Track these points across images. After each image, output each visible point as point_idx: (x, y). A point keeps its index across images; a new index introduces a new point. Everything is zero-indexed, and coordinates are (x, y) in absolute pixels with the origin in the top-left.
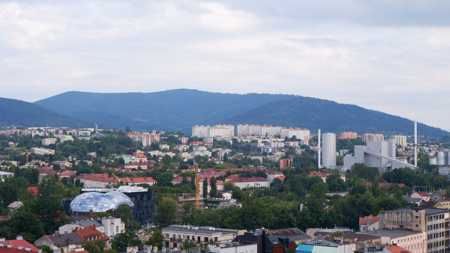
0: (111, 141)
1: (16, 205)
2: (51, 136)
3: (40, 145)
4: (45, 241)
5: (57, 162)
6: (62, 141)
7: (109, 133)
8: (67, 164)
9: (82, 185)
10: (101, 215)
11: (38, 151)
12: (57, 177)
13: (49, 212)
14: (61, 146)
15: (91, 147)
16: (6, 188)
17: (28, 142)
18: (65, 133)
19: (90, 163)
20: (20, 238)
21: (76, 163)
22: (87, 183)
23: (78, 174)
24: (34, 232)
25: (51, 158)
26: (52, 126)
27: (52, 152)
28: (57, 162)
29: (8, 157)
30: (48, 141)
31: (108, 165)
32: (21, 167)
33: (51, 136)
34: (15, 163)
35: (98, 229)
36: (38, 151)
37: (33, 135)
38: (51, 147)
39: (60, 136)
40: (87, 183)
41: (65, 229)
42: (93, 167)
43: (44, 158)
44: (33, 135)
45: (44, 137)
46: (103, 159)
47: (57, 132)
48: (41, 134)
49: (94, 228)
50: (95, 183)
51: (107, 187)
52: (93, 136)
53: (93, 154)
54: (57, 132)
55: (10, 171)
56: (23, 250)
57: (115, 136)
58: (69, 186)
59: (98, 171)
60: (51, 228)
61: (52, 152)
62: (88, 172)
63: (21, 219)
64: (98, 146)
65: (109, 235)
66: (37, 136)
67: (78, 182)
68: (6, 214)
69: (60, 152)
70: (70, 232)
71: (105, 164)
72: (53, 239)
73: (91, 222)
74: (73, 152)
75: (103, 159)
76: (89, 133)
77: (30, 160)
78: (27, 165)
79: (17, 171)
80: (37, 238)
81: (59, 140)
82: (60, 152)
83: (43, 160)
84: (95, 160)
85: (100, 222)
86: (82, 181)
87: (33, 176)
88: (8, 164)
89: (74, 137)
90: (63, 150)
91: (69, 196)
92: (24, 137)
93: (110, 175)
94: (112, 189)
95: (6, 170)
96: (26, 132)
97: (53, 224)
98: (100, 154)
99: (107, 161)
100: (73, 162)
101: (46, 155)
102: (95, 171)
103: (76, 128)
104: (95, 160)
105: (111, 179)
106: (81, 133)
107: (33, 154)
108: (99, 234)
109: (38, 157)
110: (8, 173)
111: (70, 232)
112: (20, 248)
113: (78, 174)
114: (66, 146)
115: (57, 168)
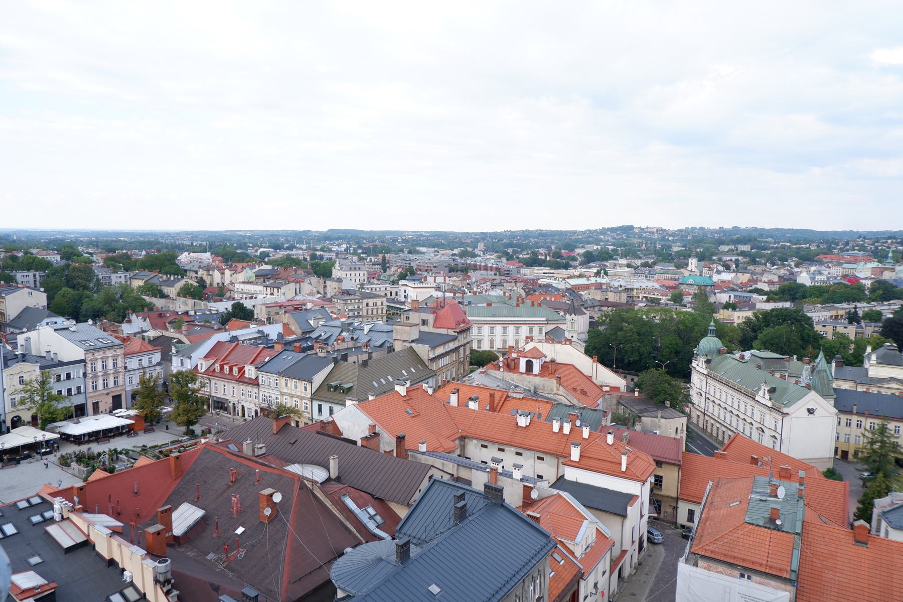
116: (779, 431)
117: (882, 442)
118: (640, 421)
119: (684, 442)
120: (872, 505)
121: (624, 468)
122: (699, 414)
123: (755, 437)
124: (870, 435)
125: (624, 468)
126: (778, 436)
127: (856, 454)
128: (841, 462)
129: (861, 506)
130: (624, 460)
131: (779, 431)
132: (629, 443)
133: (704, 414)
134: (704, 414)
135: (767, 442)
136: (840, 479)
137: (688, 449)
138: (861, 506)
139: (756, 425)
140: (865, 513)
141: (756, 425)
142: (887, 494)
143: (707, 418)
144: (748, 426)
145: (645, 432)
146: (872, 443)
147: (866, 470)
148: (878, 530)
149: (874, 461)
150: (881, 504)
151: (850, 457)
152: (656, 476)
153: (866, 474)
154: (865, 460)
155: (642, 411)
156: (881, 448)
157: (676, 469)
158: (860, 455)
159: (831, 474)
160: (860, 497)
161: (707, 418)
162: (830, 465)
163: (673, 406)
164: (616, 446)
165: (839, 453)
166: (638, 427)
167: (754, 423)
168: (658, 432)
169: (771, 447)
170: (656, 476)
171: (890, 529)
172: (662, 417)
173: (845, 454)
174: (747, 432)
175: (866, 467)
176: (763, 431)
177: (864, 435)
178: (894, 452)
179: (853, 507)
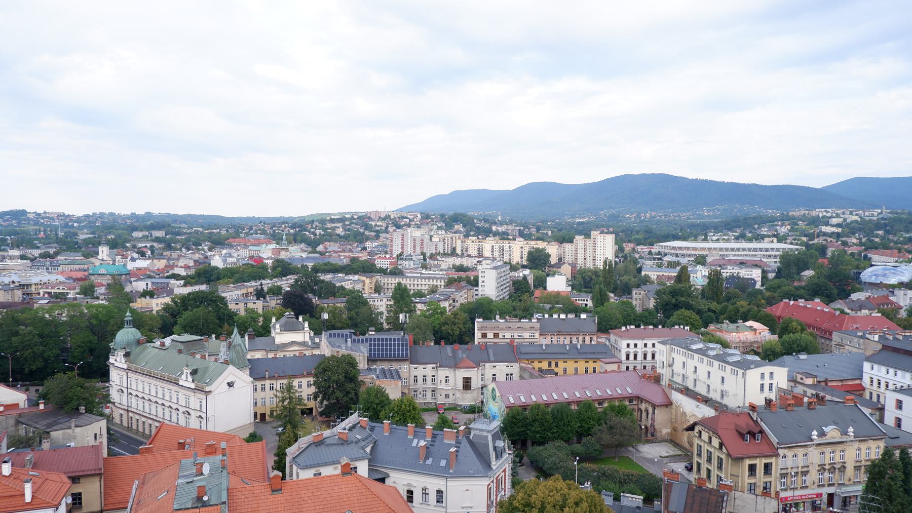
0: (900, 220)
1: (808, 273)
2: (838, 216)
3: (827, 224)
4: (839, 304)
5: (844, 239)
6: (849, 221)
7: (897, 213)
8: (854, 241)
9: (870, 259)
10: (893, 286)
11: (825, 229)
12: (845, 251)
13: (840, 281)
14: (848, 225)
15: (878, 226)
16: (798, 260)
17: (816, 222)
18: (851, 213)
19: (877, 240)
20: (817, 300)
21: (863, 240)
22: (875, 258)
23: (866, 250)
24: (828, 296)
25: (838, 236)
26: (839, 208)
27: (839, 230)
28: (844, 239)
29: (798, 233)
30: (835, 221)
31: (896, 243)
32: (811, 243)
33: (836, 218)
34: (805, 239)
35: (891, 298)
36: (825, 229)
37: (821, 215)
38: (838, 225)
39: (846, 217)
40: (875, 258)
41: (854, 296)
42: (880, 244)
43: (832, 235)
44: (821, 215)
45: (832, 217)
46: (891, 237)
47: (844, 213)
48: (829, 215)
49: (887, 297)
50: (883, 258)
51: (896, 262)
52: (880, 216)
53: (881, 232)
54: (844, 213)
55: (800, 245)
56: (822, 311)
57: (904, 216)
58: (858, 260)
59: (886, 247)
60: (845, 294)
61: (839, 230)
62: (876, 248)
63: (817, 285)
64: (886, 225)
65: (902, 304)
66: (824, 217)
67: (866, 256)
68: (799, 280)
69: (847, 230)
70: (863, 299)
71: (893, 241)
72: (846, 303)
73: (884, 292)
74: (860, 230)
75: (891, 237)
76: (876, 214)
77: (818, 237)
78: (816, 241)
79: (807, 245)
80: (832, 301)
81: (845, 220)
82: (847, 230)
83: (830, 237)
84: (883, 238)
85: (893, 292)
86: (869, 255)
87: (822, 250)
88: (798, 240)
89: (860, 217)
90: (850, 229)
91: (858, 267)
92: (813, 217)
93: (900, 250)
94: (904, 263)
95: (797, 244)
96: (815, 213)
97: (844, 290)
98: (887, 232)
99: (895, 239)
100: (860, 239)
101: (833, 233)
102: (884, 247)
103: (862, 209)
104: (883, 238)
105: (901, 255)
106: (867, 214)
107: (821, 232)
108: (892, 303)
109: (825, 234)
110: (799, 247)
111: (863, 299)
112: (819, 308)
113: (866, 250)
114: (853, 225)
115: (845, 244)
116: (204, 410)
117: (290, 398)
118: (49, 437)
119: (106, 448)
120: (285, 455)
121: (28, 498)
122: (122, 412)
123: (182, 423)
124: (279, 394)
125: (28, 498)
126: (204, 415)
127: (272, 413)
128: (261, 425)
129: (276, 458)
130: (28, 489)
131: (204, 410)
132: (35, 466)
133: (128, 411)
134: (128, 411)
135: (194, 424)
136: (261, 439)
137: (111, 453)
138: (276, 458)
139: (182, 409)
140: (280, 465)
141: (182, 409)
142: (296, 441)
143: (131, 414)
144: (174, 413)
145: (55, 449)
146: (283, 401)
147: (280, 426)
148: (291, 476)
149: (286, 416)
150: (291, 451)
151: (267, 417)
152: (73, 495)
153: (280, 429)
154: (278, 417)
155: (50, 425)
156: (289, 403)
157: (97, 479)
158: (275, 413)
159: (253, 438)
160: (275, 451)
161: (131, 414)
162: (251, 430)
163: (89, 411)
164: (16, 475)
165: (259, 416)
166: (46, 445)
167: (180, 408)
168: (72, 444)
169: (198, 428)
170: (73, 495)
171: (299, 471)
172: (77, 426)
173: (263, 416)
174: (174, 419)
175: (280, 423)
176: (189, 414)
177: (276, 396)
178: (300, 405)
179: (271, 460)
